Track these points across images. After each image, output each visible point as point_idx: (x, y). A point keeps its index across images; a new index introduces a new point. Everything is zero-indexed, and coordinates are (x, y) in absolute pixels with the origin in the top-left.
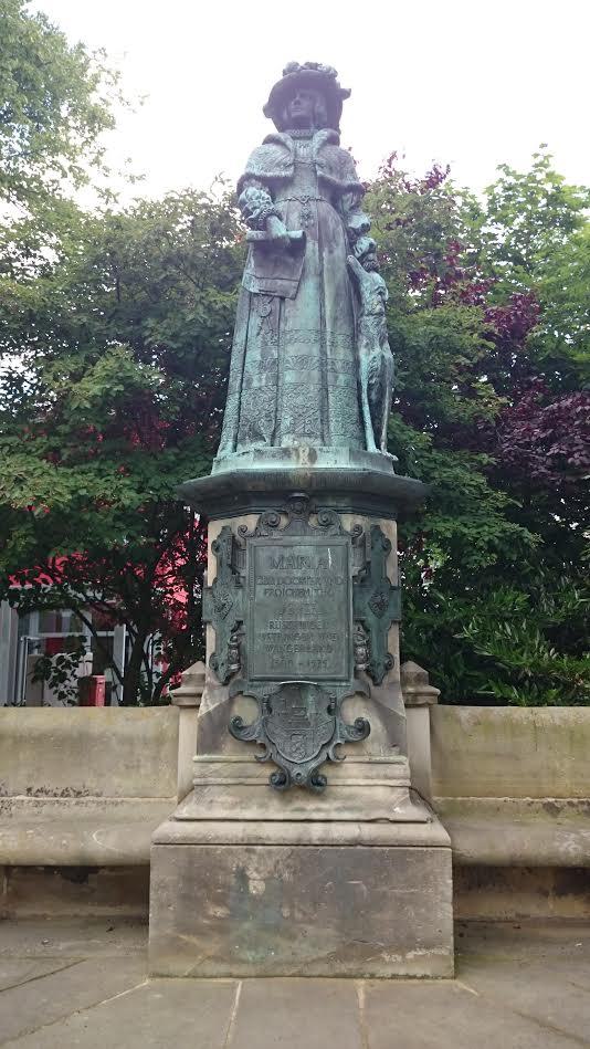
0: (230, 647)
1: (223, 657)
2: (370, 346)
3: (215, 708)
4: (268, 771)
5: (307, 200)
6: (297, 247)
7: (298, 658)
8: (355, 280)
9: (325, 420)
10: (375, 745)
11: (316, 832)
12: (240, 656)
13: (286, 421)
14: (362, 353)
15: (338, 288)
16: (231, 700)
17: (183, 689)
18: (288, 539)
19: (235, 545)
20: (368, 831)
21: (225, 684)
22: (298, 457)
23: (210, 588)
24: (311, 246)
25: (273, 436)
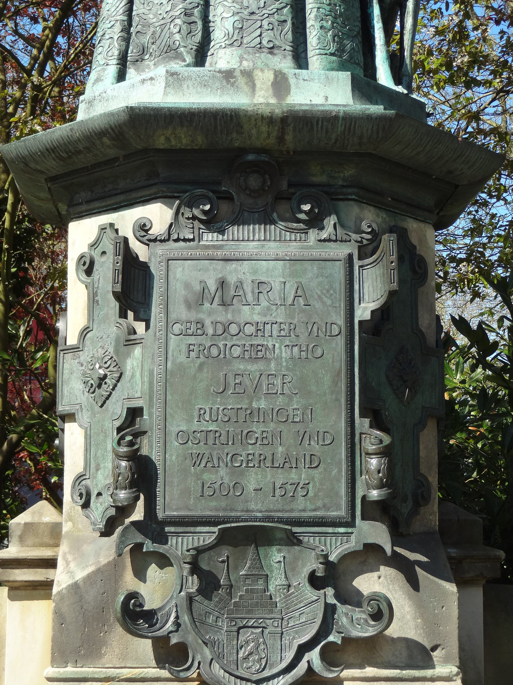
0: (118, 456)
1: (102, 479)
3: (89, 577)
7: (252, 481)
12: (142, 476)
21: (107, 532)
22: (253, 87)
23: (75, 349)
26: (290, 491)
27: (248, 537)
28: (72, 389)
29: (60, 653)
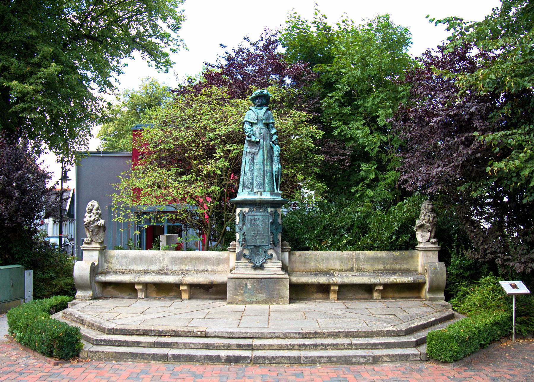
1: (241, 240)
2: (275, 165)
4: (251, 265)
5: (261, 129)
6: (258, 143)
7: (258, 241)
8: (272, 148)
9: (264, 184)
10: (274, 260)
13: (255, 184)
14: (274, 166)
15: (268, 151)
16: (243, 250)
17: (230, 247)
18: (256, 214)
19: (244, 215)
24: (261, 141)
25: (252, 188)
26: (262, 242)
27: (257, 248)
28: (237, 229)
29: (237, 259)
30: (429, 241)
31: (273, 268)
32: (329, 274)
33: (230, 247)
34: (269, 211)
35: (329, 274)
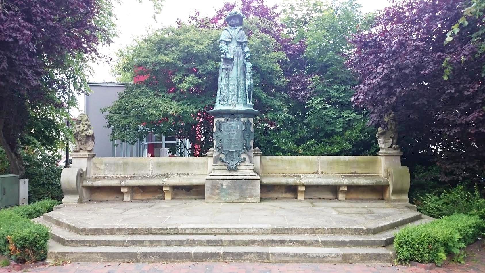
1: (218, 146)
4: (227, 167)
5: (234, 47)
6: (232, 59)
7: (232, 146)
8: (245, 65)
9: (238, 97)
11: (235, 177)
12: (221, 146)
13: (230, 98)
16: (219, 154)
19: (220, 124)
20: (245, 177)
24: (235, 58)
26: (236, 147)
27: (232, 152)
29: (214, 163)
30: (391, 147)
31: (246, 170)
32: (296, 176)
33: (209, 153)
34: (242, 120)
35: (296, 176)
